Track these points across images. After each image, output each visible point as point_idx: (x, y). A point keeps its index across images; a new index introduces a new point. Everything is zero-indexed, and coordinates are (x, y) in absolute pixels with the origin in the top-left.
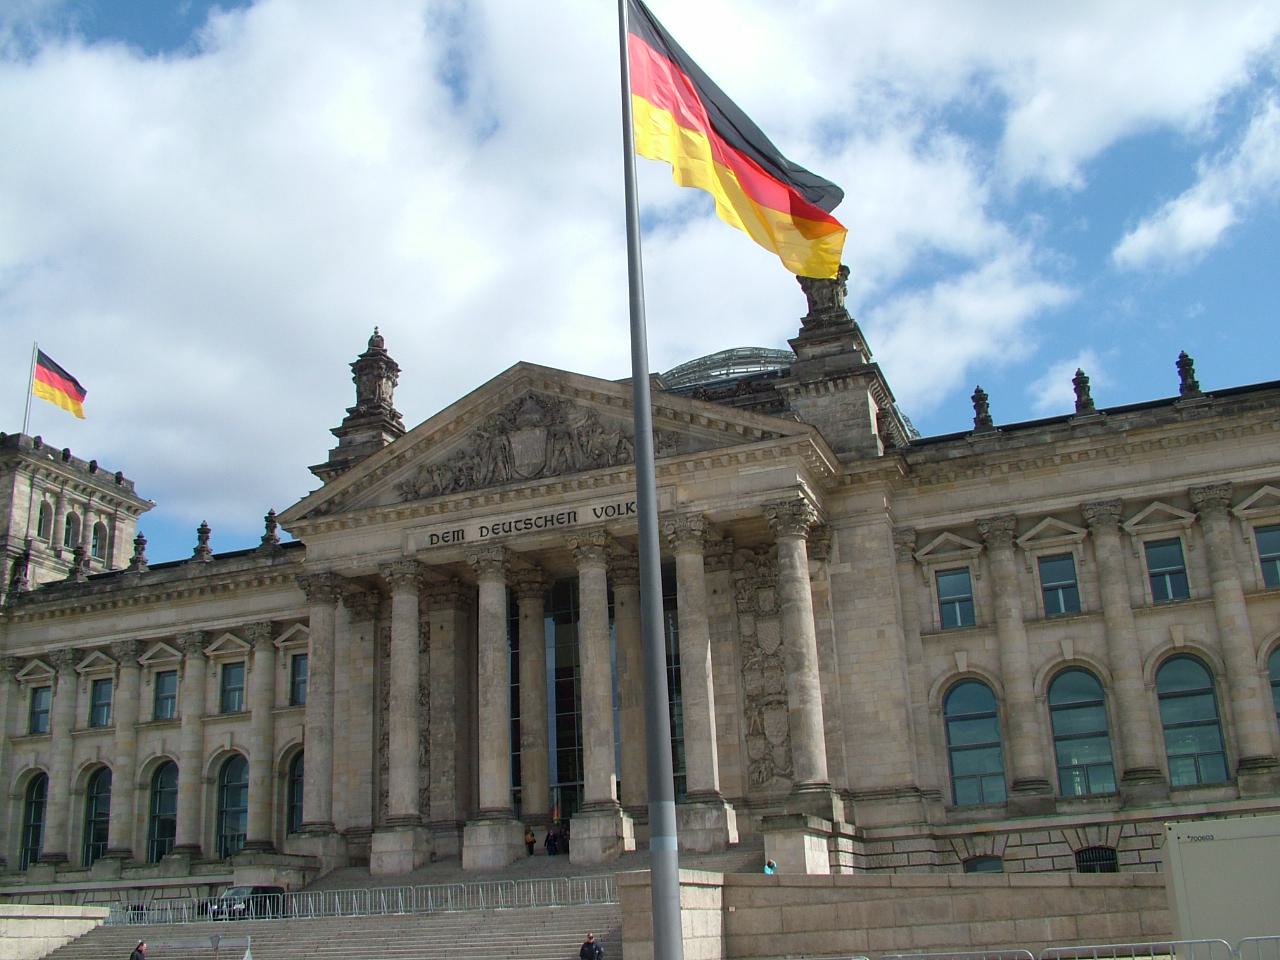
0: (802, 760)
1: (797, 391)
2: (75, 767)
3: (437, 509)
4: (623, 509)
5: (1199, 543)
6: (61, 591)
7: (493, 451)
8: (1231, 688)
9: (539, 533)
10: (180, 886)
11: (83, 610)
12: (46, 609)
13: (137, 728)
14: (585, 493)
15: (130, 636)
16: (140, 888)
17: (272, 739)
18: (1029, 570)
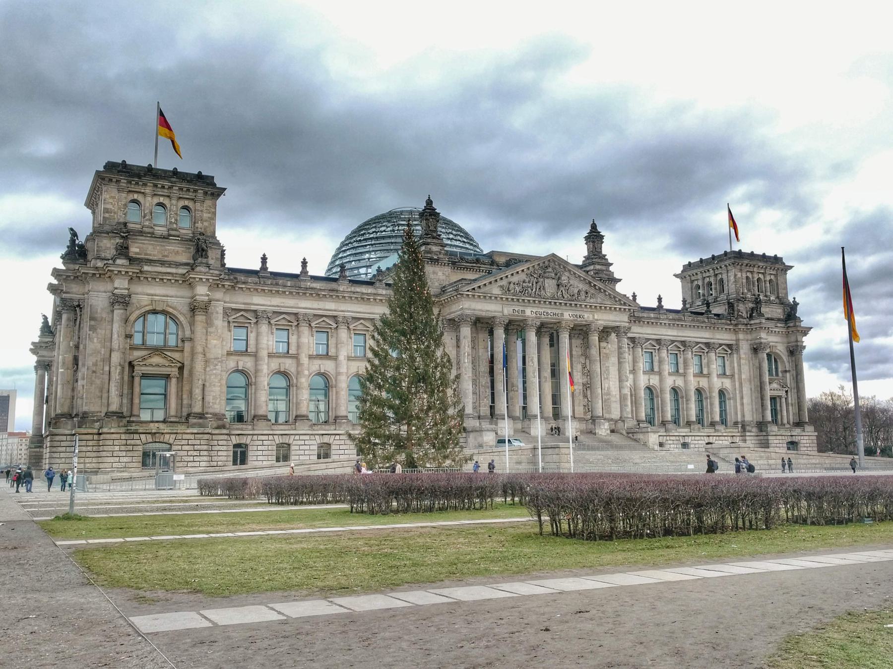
5: (682, 356)
6: (259, 278)
7: (540, 283)
8: (687, 401)
12: (260, 288)
13: (311, 357)
14: (570, 308)
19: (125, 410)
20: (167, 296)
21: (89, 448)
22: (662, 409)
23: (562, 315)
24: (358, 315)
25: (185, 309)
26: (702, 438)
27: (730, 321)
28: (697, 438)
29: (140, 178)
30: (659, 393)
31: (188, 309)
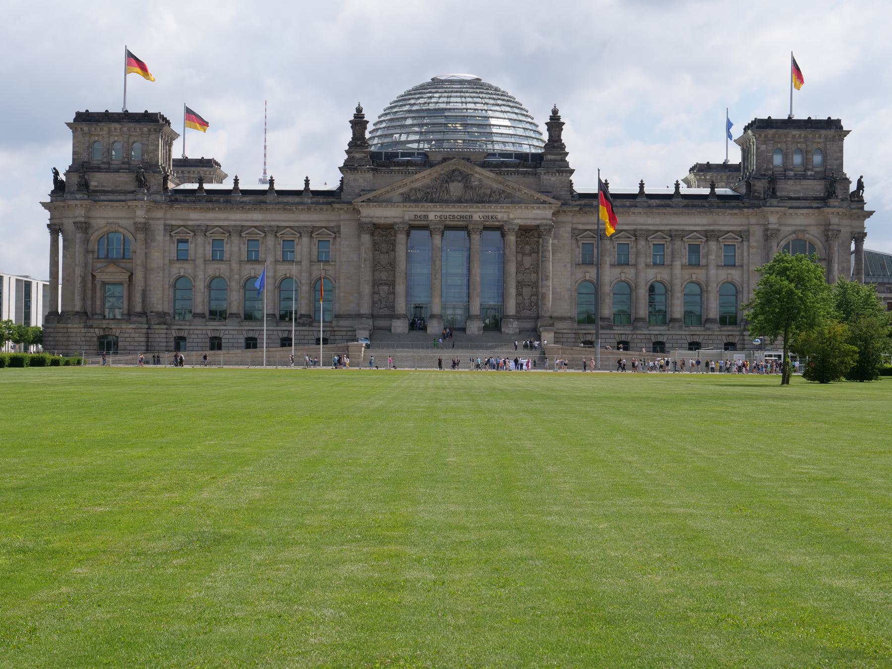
0: (545, 309)
1: (545, 173)
2: (206, 277)
3: (420, 207)
4: (490, 218)
5: (670, 247)
7: (443, 189)
8: (672, 296)
9: (458, 221)
10: (273, 330)
11: (213, 209)
13: (240, 262)
14: (477, 210)
15: (238, 223)
16: (253, 330)
17: (311, 274)
18: (614, 247)
19: (89, 310)
20: (118, 218)
21: (65, 339)
22: (636, 306)
23: (471, 217)
24: (284, 224)
25: (132, 229)
26: (684, 337)
27: (743, 203)
28: (674, 337)
29: (97, 125)
30: (634, 289)
31: (133, 228)
